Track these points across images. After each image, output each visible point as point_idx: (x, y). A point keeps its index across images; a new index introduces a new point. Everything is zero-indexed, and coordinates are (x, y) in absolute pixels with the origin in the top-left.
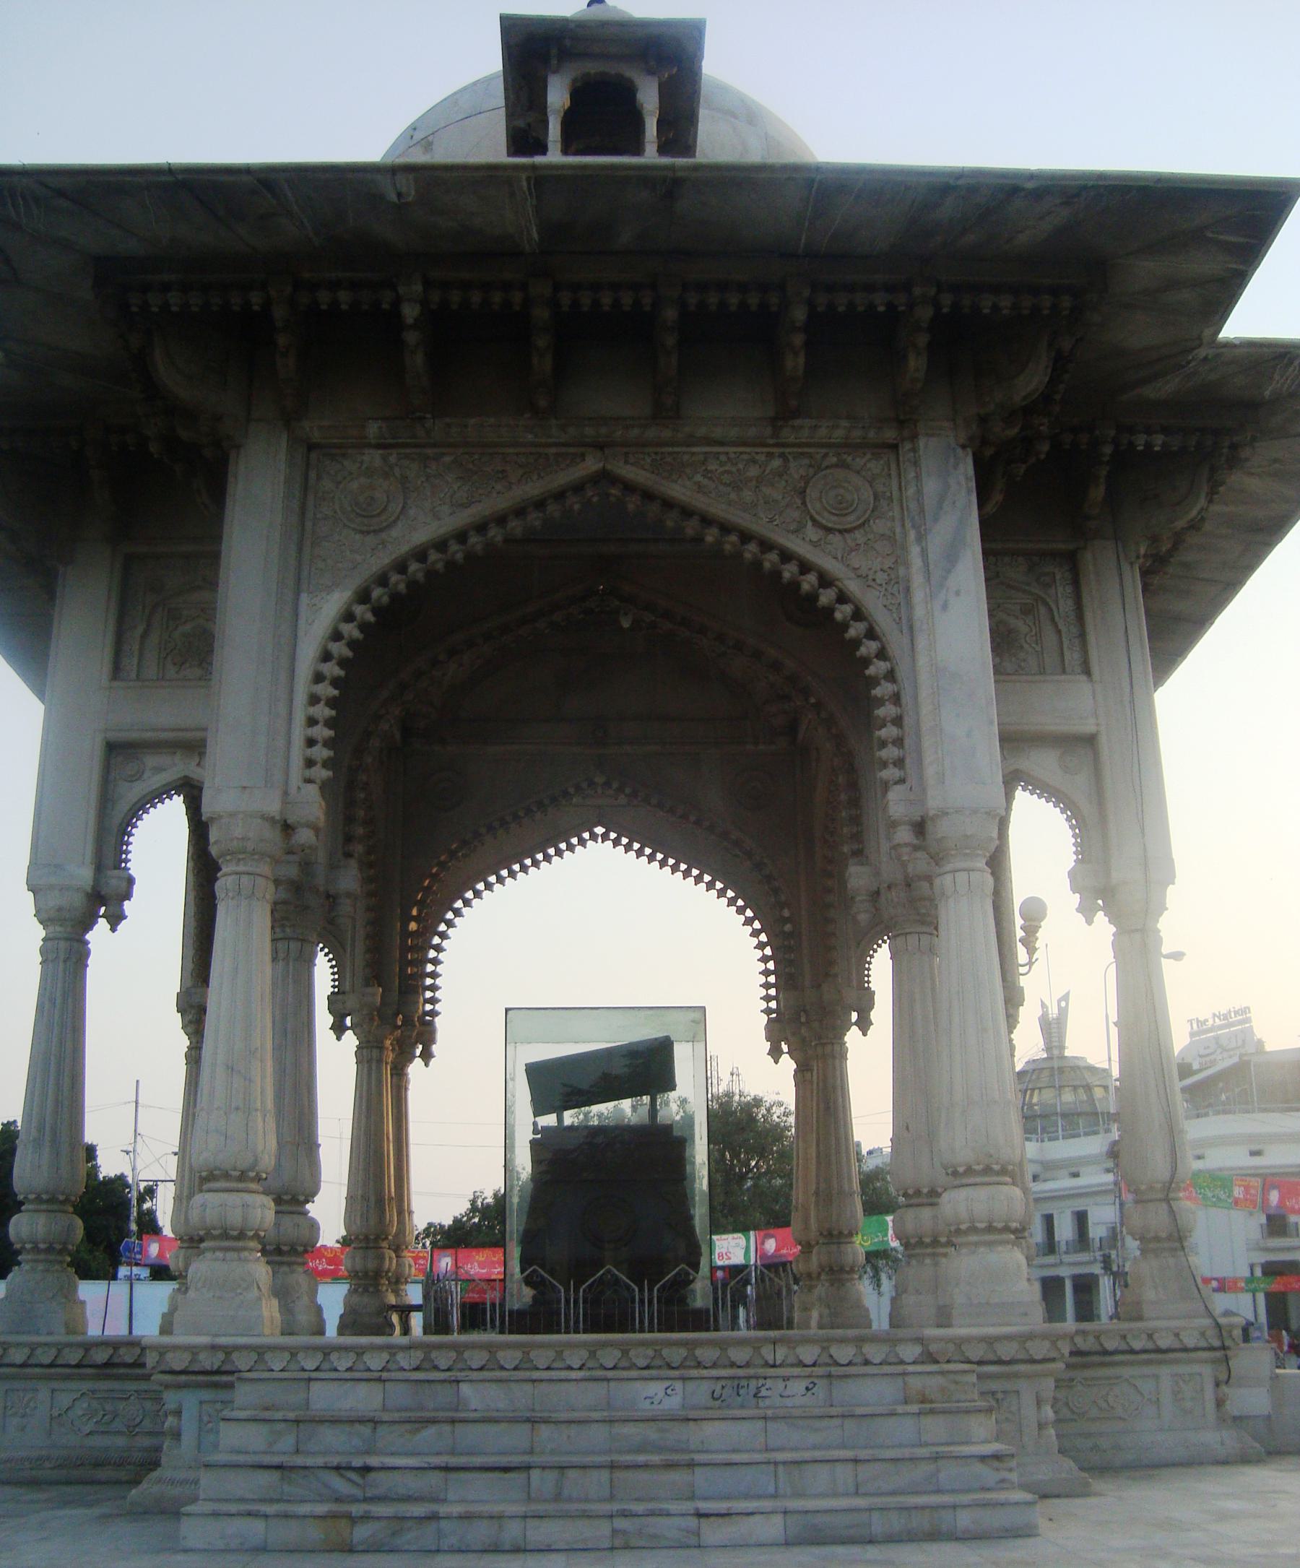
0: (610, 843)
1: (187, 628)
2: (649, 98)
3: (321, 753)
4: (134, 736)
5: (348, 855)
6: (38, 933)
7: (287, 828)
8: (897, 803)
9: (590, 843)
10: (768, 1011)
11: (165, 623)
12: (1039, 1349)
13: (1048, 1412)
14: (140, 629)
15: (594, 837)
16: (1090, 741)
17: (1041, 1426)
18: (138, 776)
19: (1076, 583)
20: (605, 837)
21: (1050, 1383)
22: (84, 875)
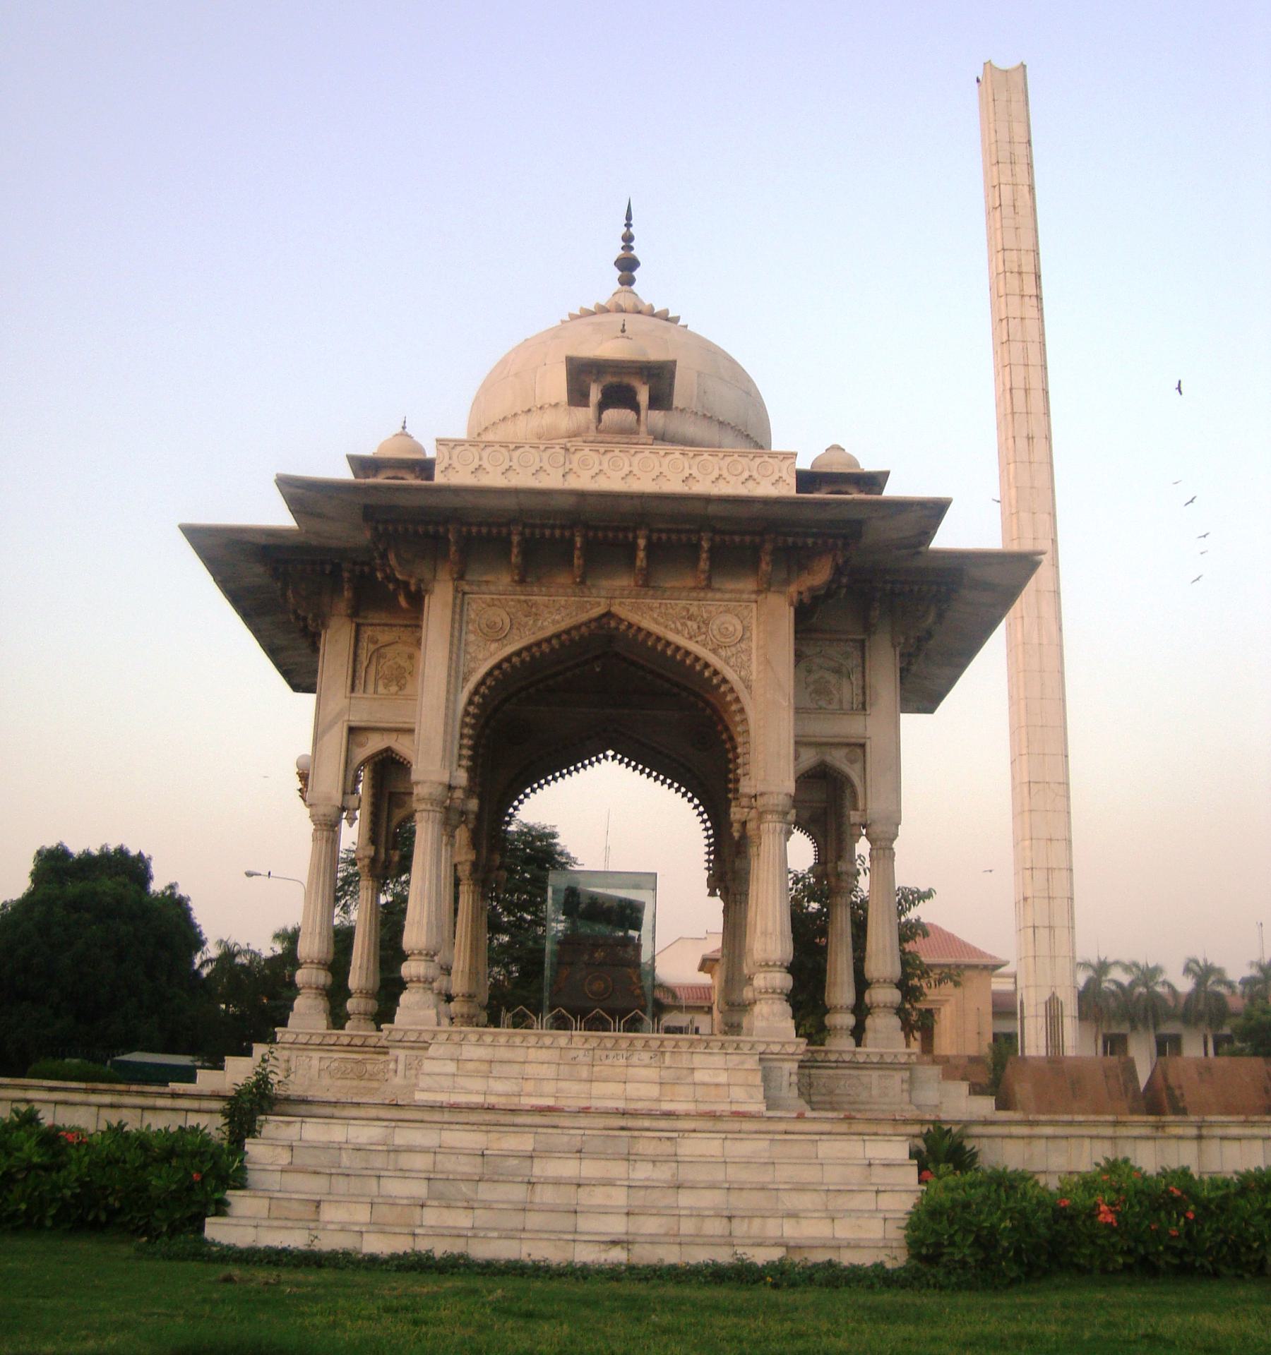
0: (616, 762)
1: (388, 663)
2: (643, 396)
3: (466, 752)
4: (363, 724)
6: (310, 827)
7: (450, 788)
8: (746, 787)
9: (603, 761)
10: (708, 869)
11: (380, 670)
12: (791, 1049)
13: (794, 1078)
14: (365, 664)
15: (606, 757)
16: (863, 746)
18: (362, 745)
19: (863, 658)
20: (614, 758)
21: (796, 1065)
22: (337, 798)
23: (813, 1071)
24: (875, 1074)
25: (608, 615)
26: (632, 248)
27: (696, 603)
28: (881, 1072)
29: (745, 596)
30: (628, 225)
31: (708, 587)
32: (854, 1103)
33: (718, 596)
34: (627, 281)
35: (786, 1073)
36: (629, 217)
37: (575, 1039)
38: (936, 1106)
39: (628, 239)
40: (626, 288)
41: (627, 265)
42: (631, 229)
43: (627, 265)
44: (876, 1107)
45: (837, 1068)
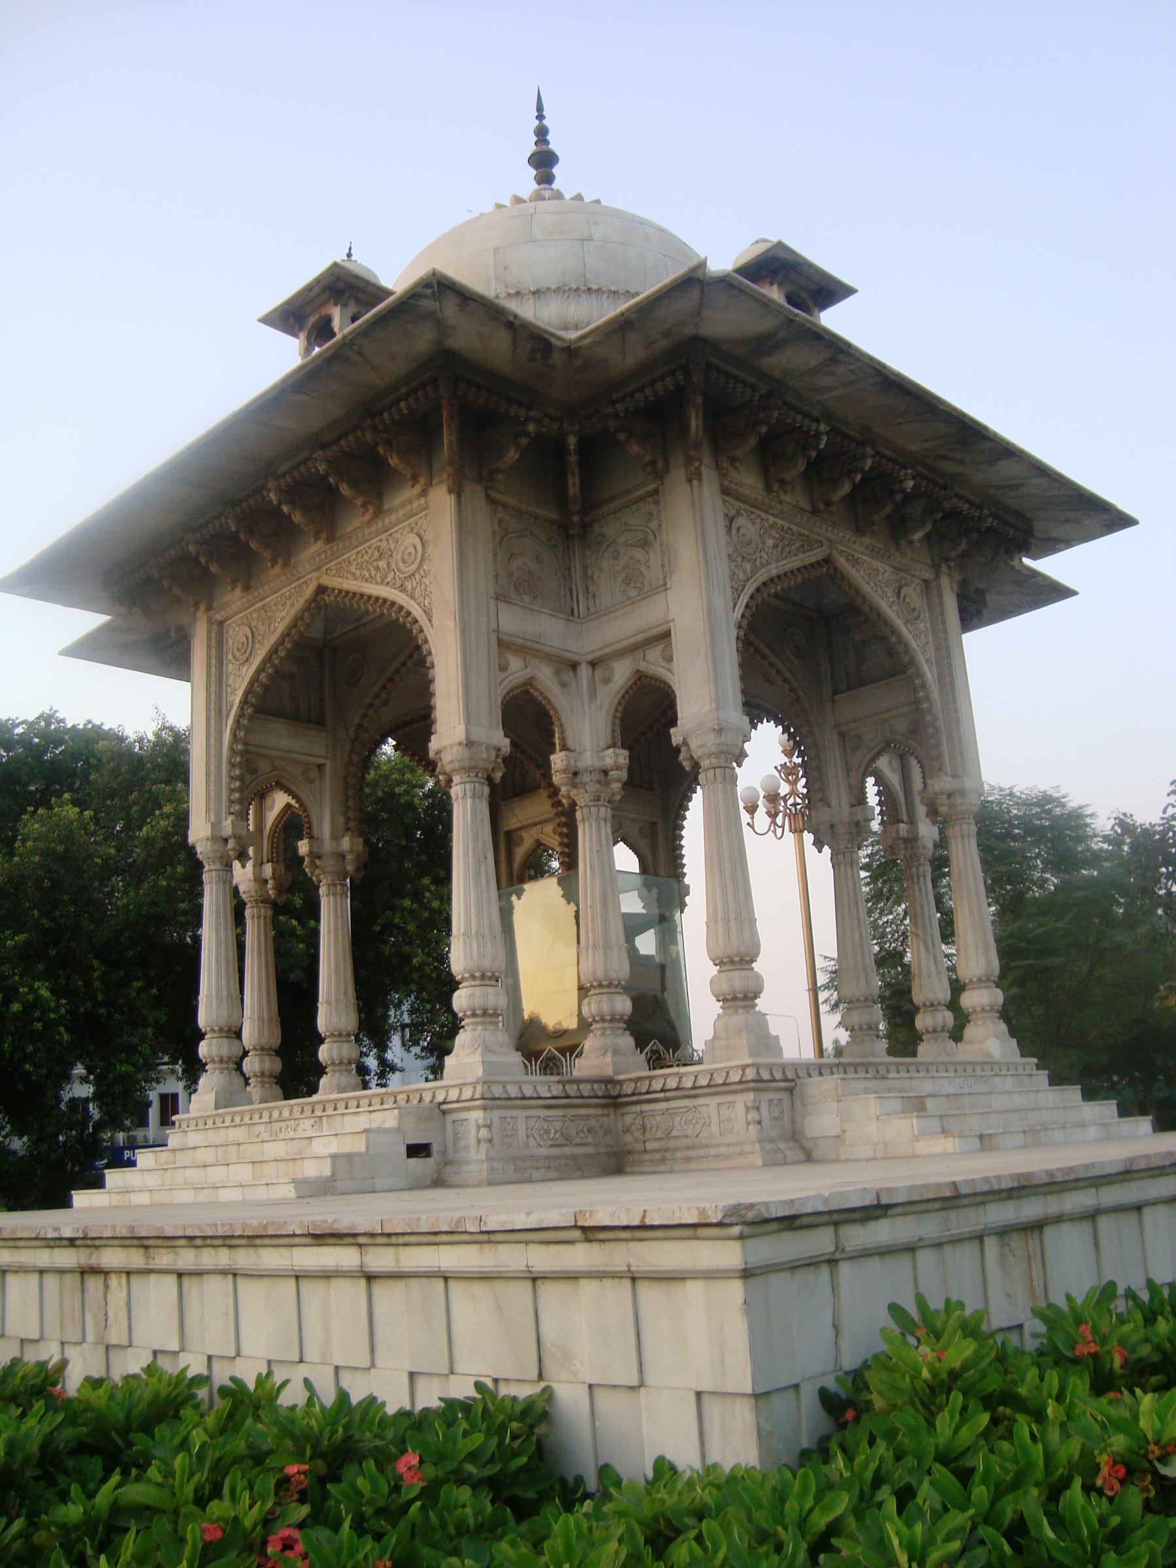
5: (348, 829)
17: (479, 1142)
23: (645, 1107)
24: (713, 1102)
25: (322, 590)
26: (547, 143)
27: (384, 536)
28: (719, 1099)
29: (415, 504)
30: (540, 117)
31: (379, 512)
32: (693, 1147)
33: (394, 517)
34: (545, 178)
35: (472, 1126)
36: (540, 108)
37: (296, 1108)
38: (838, 1137)
39: (541, 133)
40: (546, 186)
41: (544, 162)
42: (544, 122)
43: (544, 162)
44: (713, 1151)
45: (667, 1099)
